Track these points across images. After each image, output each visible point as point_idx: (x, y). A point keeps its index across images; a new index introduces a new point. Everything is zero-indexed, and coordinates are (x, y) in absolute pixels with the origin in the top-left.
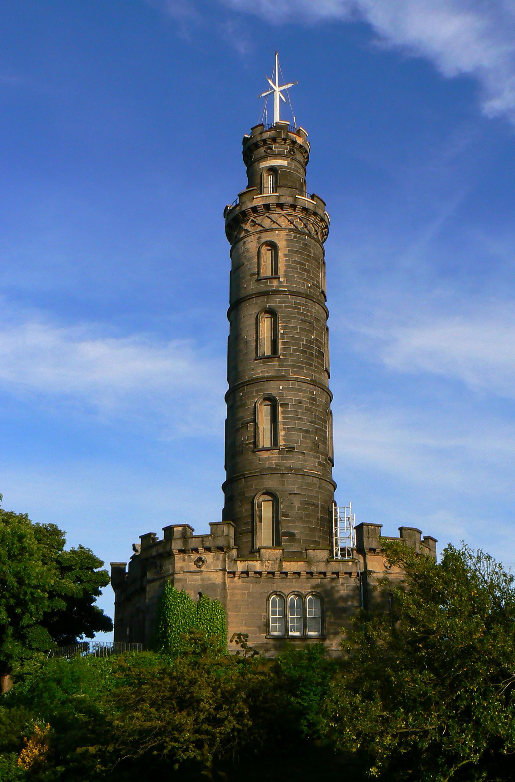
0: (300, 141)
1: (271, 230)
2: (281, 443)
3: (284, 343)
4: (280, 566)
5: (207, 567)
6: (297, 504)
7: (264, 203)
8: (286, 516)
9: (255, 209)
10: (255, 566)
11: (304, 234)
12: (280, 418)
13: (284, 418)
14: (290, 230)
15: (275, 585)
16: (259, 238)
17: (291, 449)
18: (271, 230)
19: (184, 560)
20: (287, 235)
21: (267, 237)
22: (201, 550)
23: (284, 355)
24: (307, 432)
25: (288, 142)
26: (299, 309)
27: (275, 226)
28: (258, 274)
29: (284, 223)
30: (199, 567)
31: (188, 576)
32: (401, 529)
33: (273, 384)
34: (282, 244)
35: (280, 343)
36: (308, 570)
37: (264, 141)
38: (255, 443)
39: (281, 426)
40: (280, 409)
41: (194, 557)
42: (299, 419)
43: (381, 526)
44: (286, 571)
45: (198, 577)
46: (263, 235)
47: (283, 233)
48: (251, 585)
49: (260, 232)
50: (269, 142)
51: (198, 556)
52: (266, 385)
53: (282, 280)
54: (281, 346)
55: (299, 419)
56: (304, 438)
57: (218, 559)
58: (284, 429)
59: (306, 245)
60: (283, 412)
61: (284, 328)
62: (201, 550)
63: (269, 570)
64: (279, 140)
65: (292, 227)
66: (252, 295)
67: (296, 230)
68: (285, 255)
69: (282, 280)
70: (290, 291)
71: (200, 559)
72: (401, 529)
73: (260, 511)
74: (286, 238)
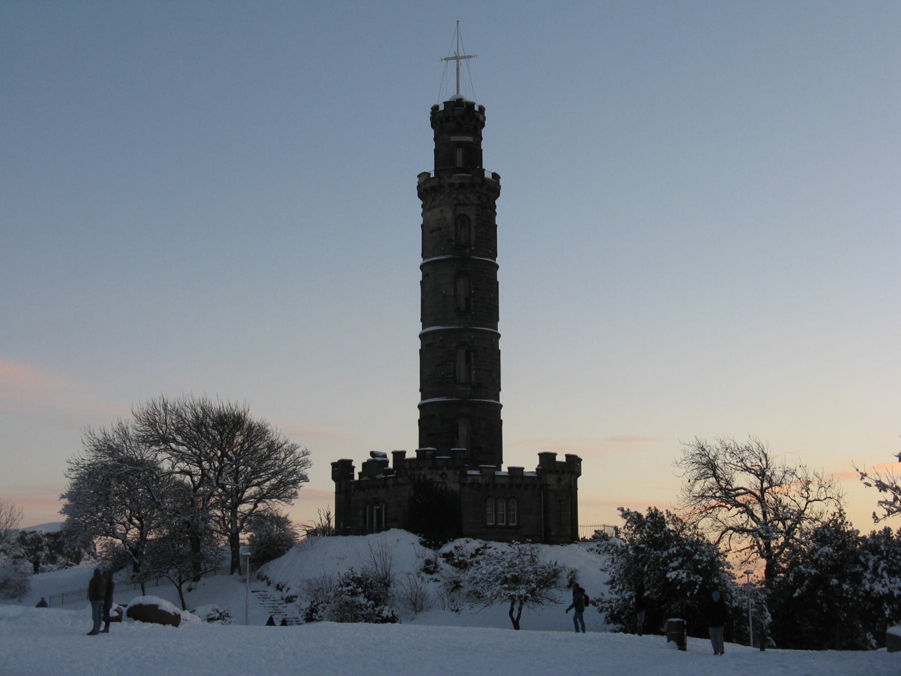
2: (473, 380)
18: (465, 204)
22: (445, 468)
39: (473, 367)
40: (472, 354)
41: (439, 472)
71: (444, 473)
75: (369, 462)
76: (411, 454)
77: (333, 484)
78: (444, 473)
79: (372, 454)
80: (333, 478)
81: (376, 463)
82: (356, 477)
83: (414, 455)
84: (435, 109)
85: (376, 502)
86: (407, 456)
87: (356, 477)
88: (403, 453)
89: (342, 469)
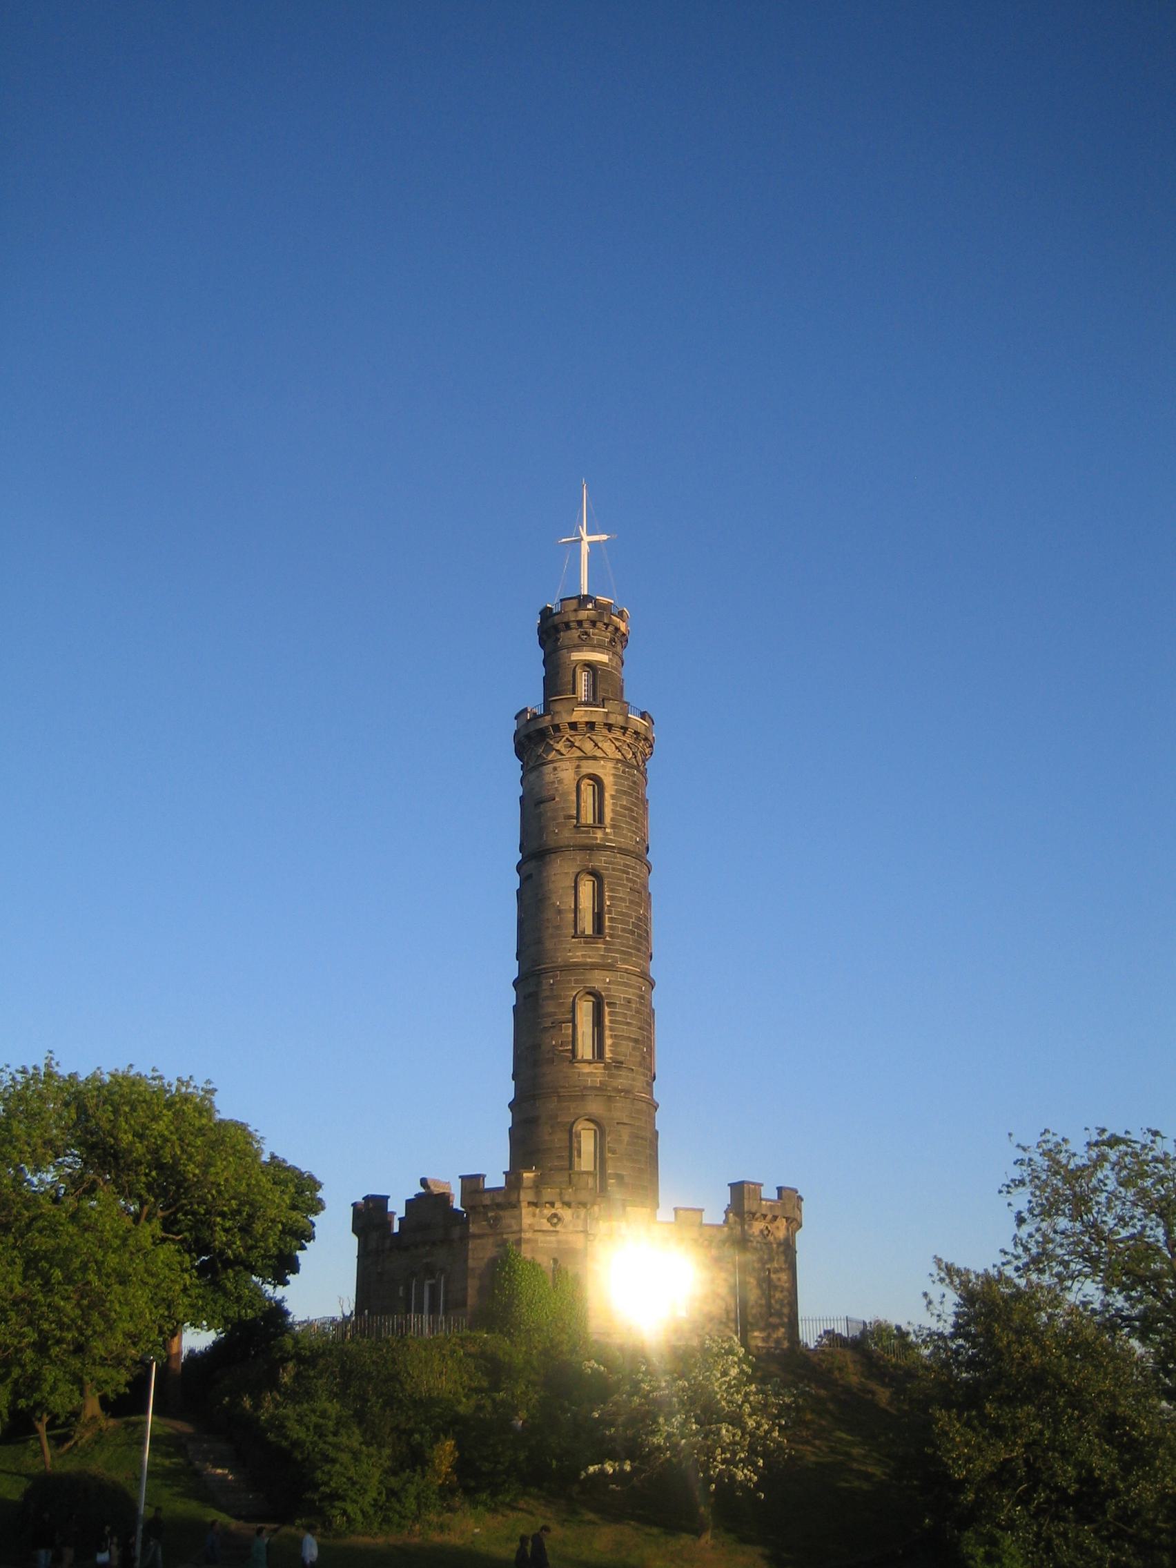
0: (623, 627)
1: (595, 758)
2: (608, 1055)
3: (611, 919)
5: (565, 1227)
6: (626, 1138)
7: (587, 719)
8: (614, 1152)
9: (573, 726)
11: (632, 767)
12: (607, 1022)
13: (611, 1021)
14: (618, 761)
16: (578, 767)
17: (618, 1064)
18: (595, 758)
19: (534, 1215)
21: (589, 767)
23: (611, 936)
24: (636, 1041)
25: (611, 628)
26: (628, 873)
27: (599, 753)
28: (578, 818)
29: (609, 748)
30: (554, 1225)
31: (540, 1237)
32: (780, 1189)
33: (597, 974)
34: (608, 781)
37: (580, 623)
38: (573, 1052)
39: (607, 1033)
41: (548, 1212)
42: (628, 1024)
43: (761, 1185)
45: (553, 1238)
46: (584, 763)
47: (610, 765)
49: (580, 758)
50: (586, 625)
51: (553, 1211)
52: (589, 975)
53: (608, 830)
54: (607, 924)
55: (628, 1024)
56: (634, 1049)
57: (578, 1217)
59: (634, 782)
61: (611, 898)
62: (558, 1205)
64: (599, 625)
65: (619, 757)
66: (569, 846)
67: (624, 762)
68: (613, 797)
69: (608, 830)
70: (619, 848)
71: (555, 1215)
72: (780, 1189)
73: (579, 1142)
75: (419, 1196)
76: (495, 1179)
77: (355, 1239)
78: (555, 1215)
79: (424, 1183)
80: (355, 1230)
81: (429, 1203)
82: (396, 1229)
83: (501, 1182)
85: (430, 1271)
86: (488, 1184)
87: (396, 1229)
88: (478, 1178)
89: (369, 1216)
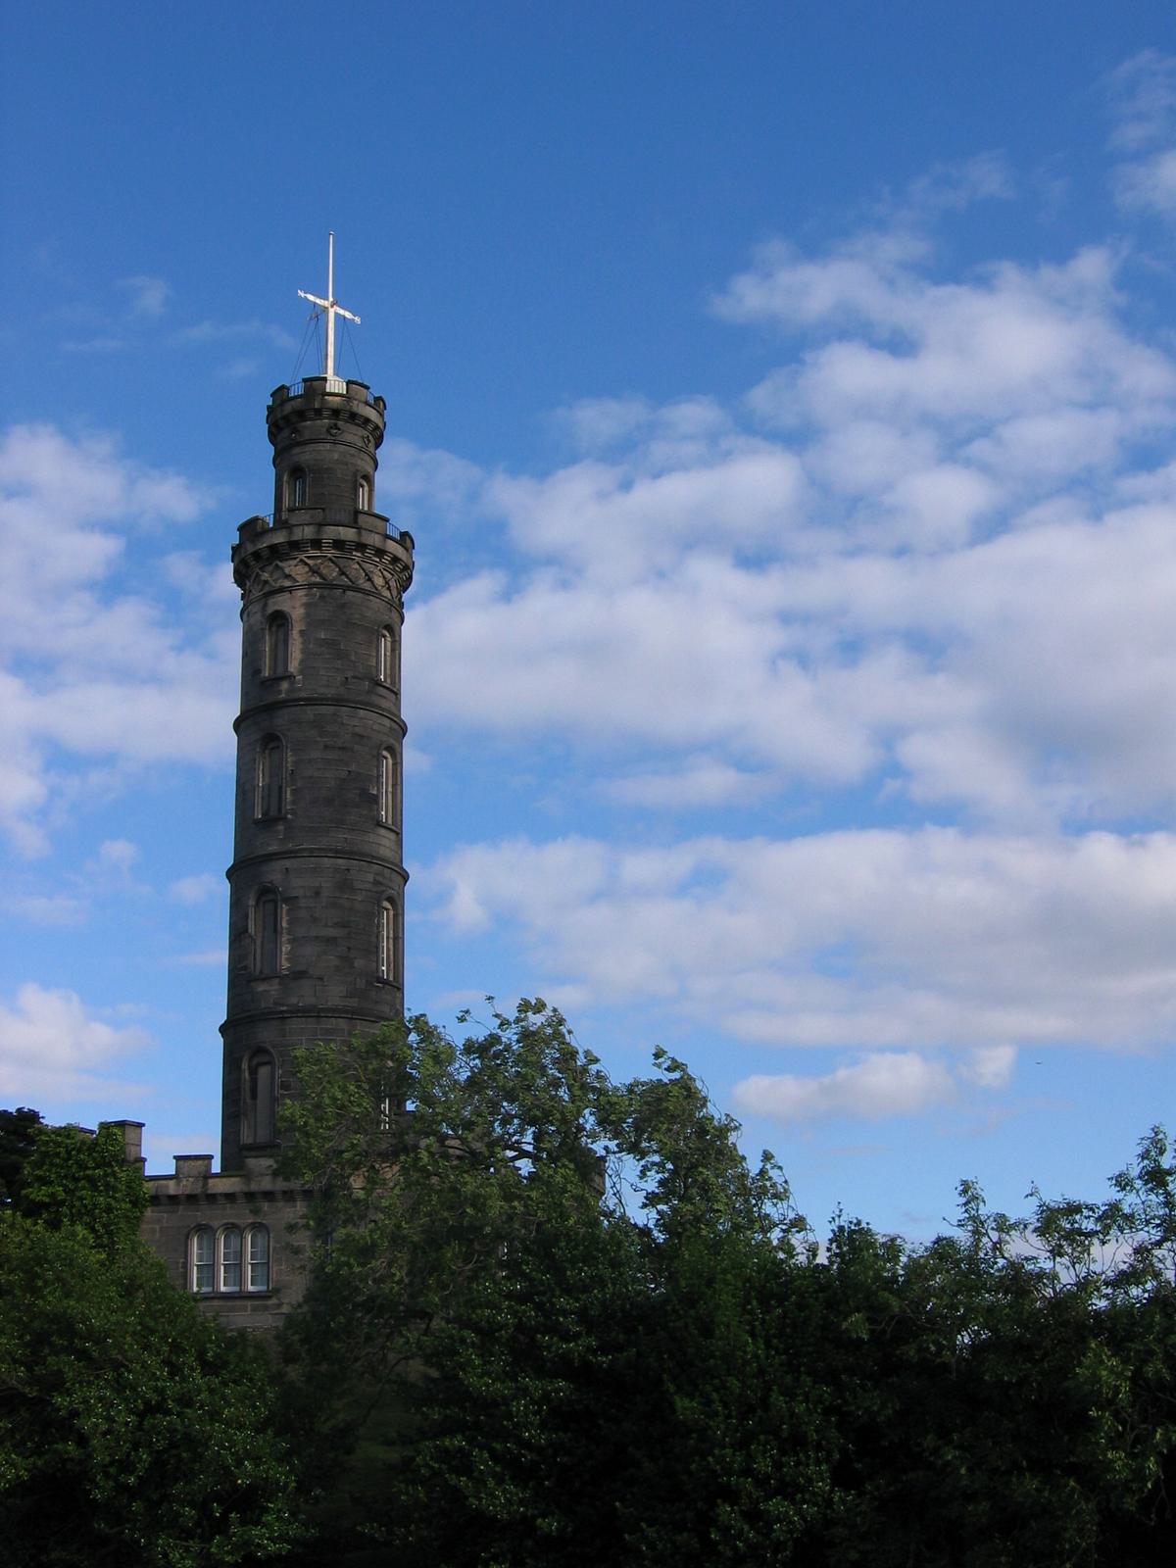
1: (282, 590)
3: (294, 792)
4: (205, 1184)
10: (167, 1186)
13: (290, 922)
14: (311, 586)
15: (199, 1214)
17: (298, 975)
18: (282, 590)
20: (306, 595)
24: (331, 941)
27: (287, 583)
35: (288, 793)
36: (245, 1189)
44: (213, 1192)
48: (165, 1215)
58: (289, 941)
60: (288, 910)
63: (188, 1192)
68: (302, 632)
74: (305, 600)
84: (280, 394)
